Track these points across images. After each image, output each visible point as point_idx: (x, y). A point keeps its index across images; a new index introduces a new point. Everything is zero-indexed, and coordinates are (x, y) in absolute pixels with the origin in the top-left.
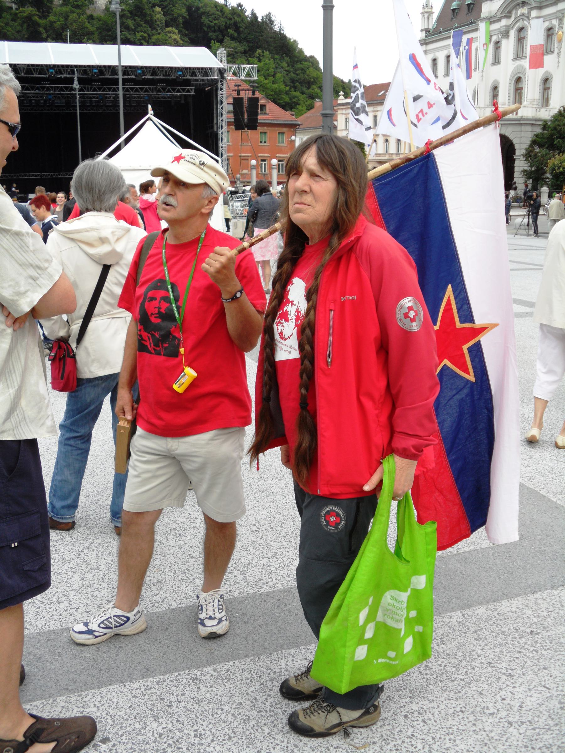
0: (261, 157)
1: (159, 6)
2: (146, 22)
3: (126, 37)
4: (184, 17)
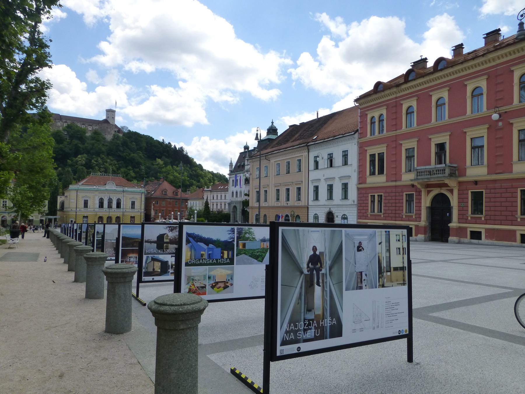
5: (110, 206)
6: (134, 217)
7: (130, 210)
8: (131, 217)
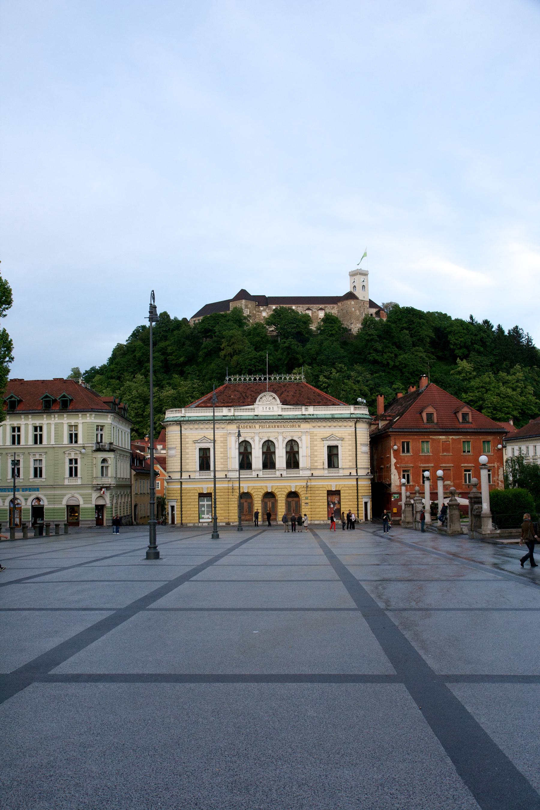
0: (464, 467)
1: (406, 329)
2: (395, 344)
3: (374, 358)
4: (431, 338)
5: (269, 463)
6: (337, 493)
7: (326, 473)
8: (330, 493)
